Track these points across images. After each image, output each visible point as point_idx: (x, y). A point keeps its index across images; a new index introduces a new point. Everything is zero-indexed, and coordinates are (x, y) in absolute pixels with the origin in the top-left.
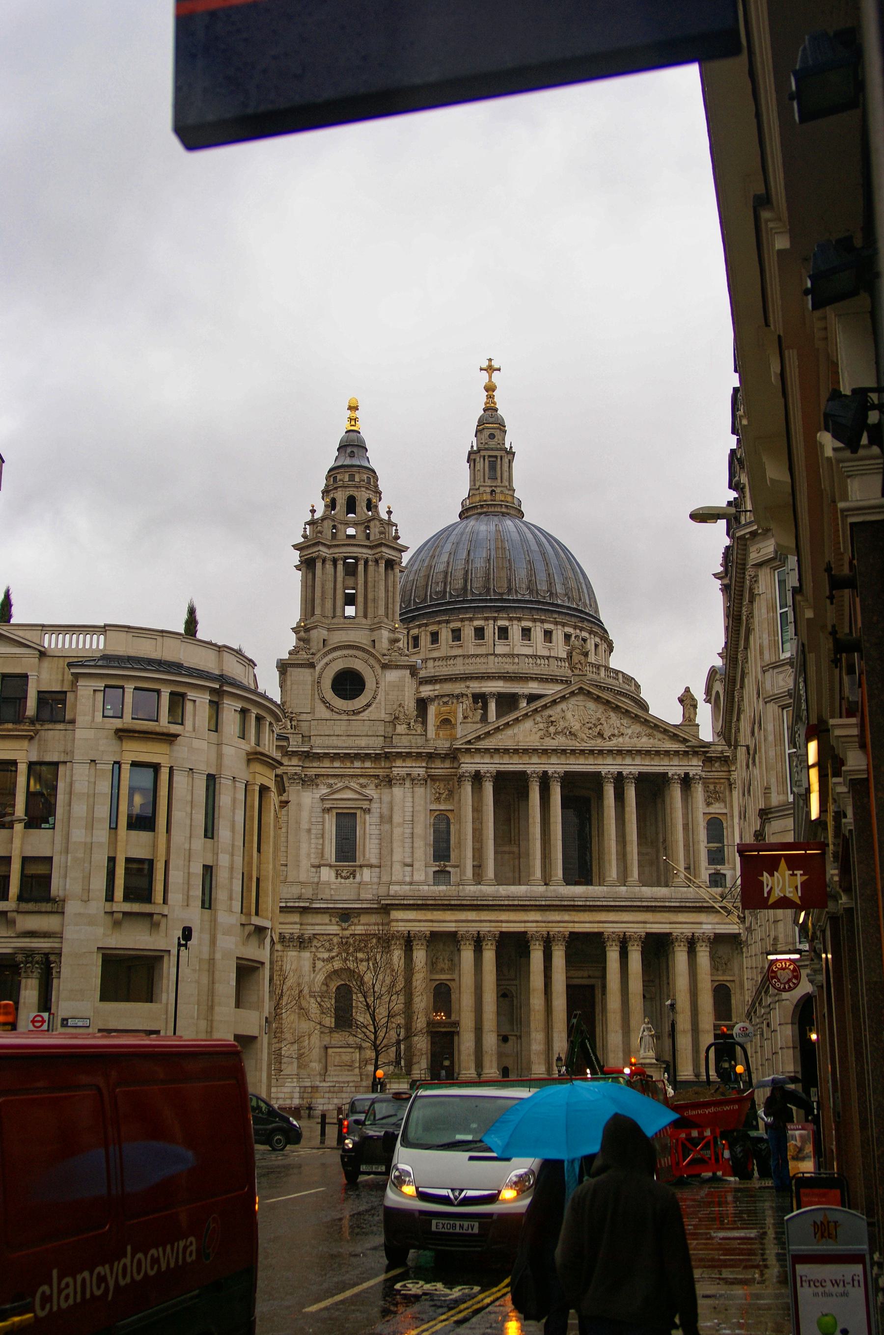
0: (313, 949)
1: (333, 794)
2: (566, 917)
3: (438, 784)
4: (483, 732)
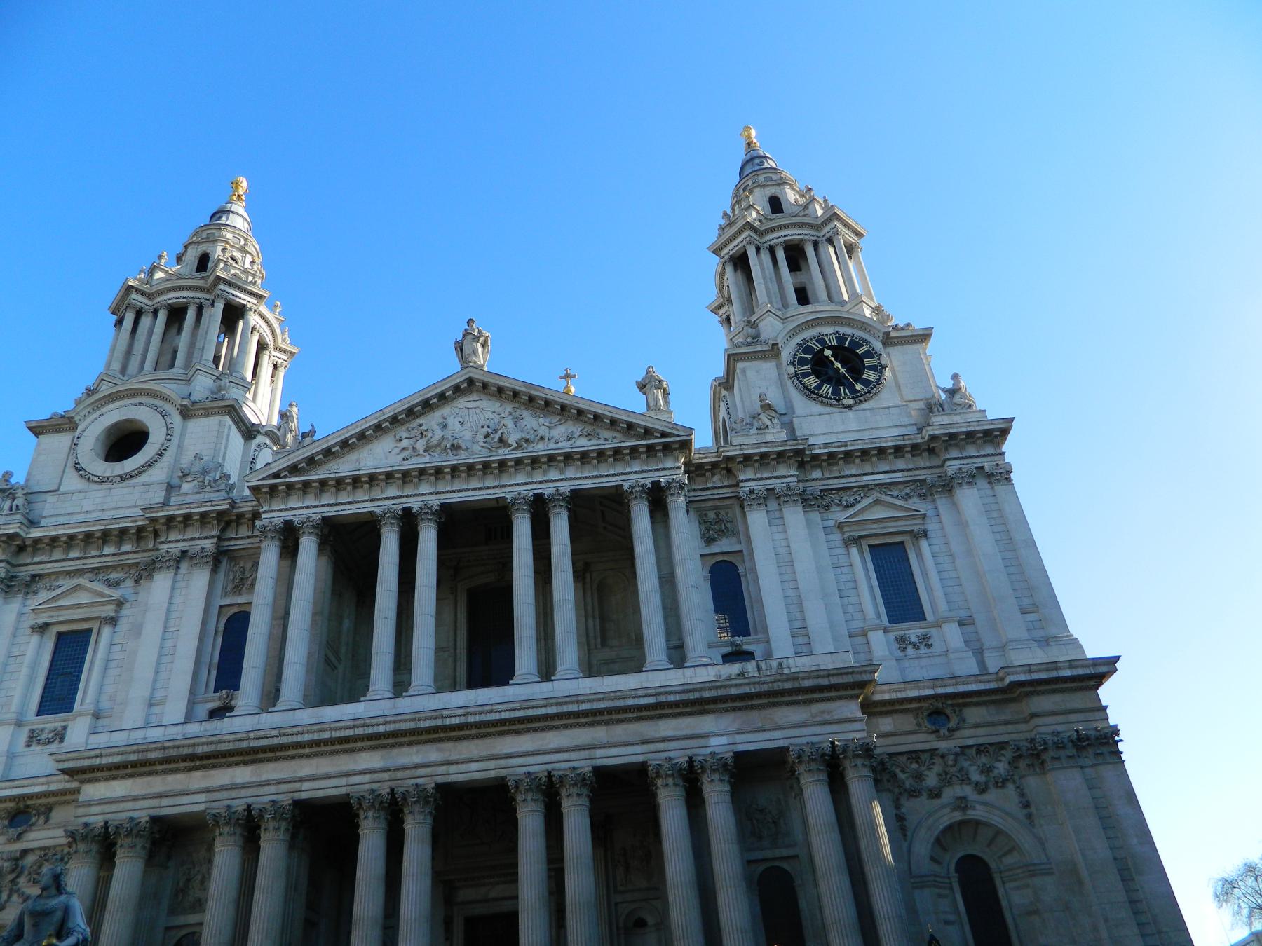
1: (54, 599)
2: (432, 753)
4: (302, 457)
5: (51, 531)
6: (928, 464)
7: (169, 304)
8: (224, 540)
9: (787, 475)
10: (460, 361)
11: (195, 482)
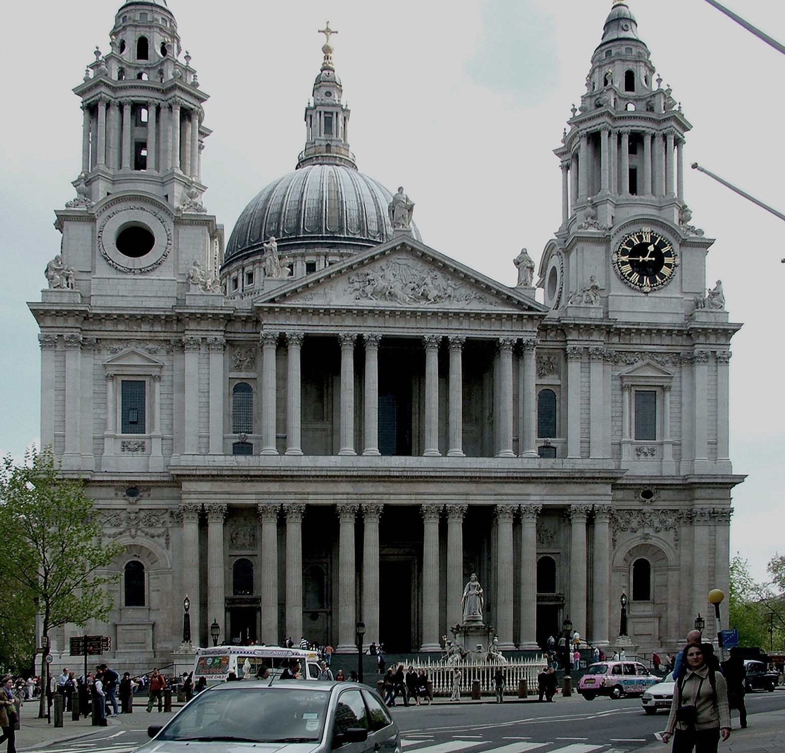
2: (381, 488)
3: (238, 349)
4: (290, 289)
8: (227, 332)
9: (597, 341)
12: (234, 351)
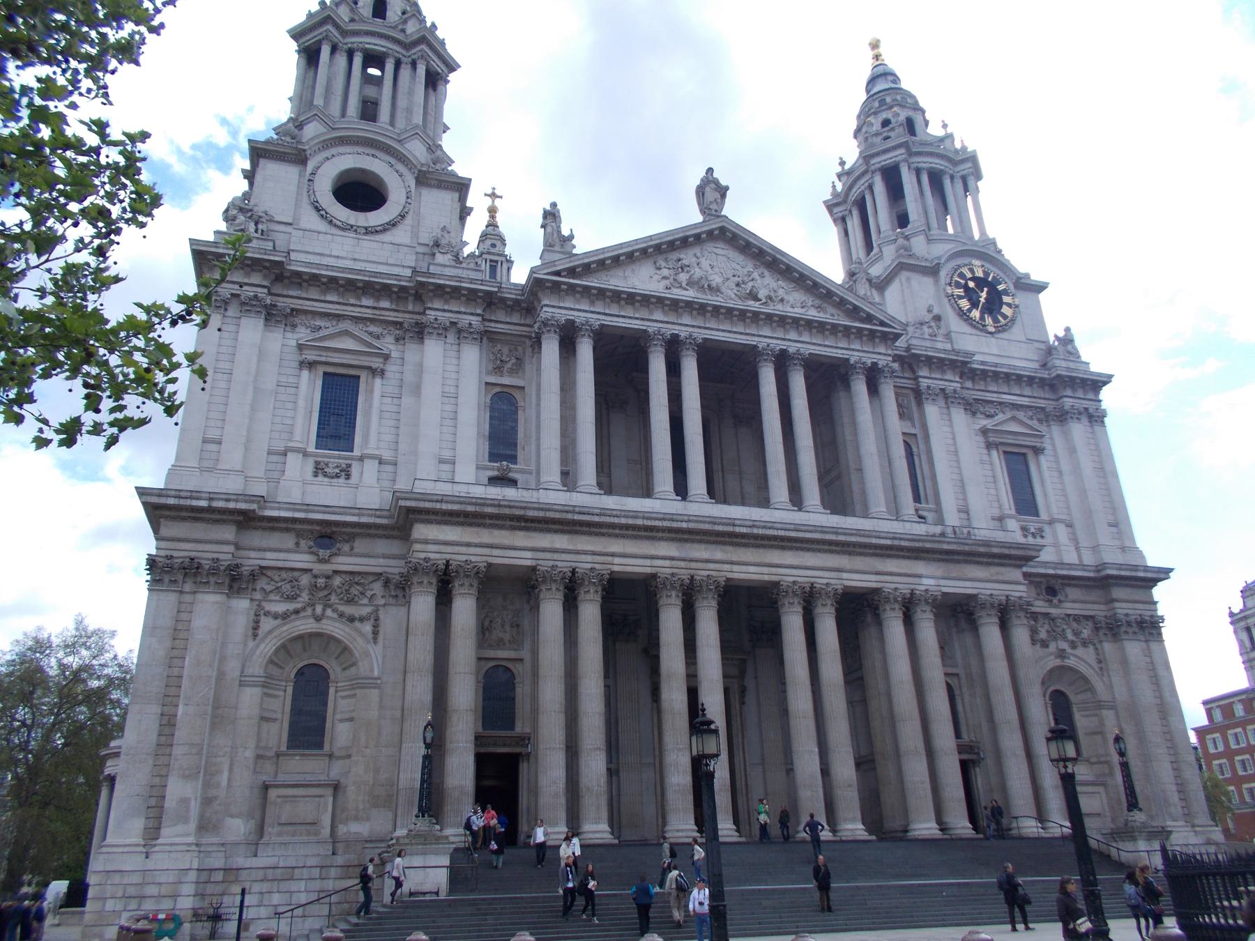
0: (258, 596)
2: (718, 553)
3: (499, 346)
4: (581, 262)
5: (312, 268)
6: (1047, 396)
7: (366, 49)
9: (951, 381)
10: (699, 204)
11: (449, 256)
12: (493, 347)
